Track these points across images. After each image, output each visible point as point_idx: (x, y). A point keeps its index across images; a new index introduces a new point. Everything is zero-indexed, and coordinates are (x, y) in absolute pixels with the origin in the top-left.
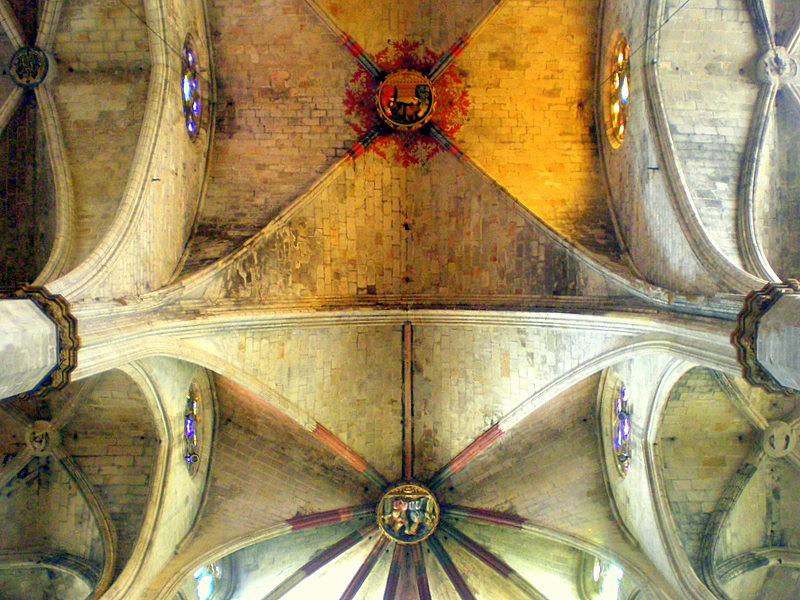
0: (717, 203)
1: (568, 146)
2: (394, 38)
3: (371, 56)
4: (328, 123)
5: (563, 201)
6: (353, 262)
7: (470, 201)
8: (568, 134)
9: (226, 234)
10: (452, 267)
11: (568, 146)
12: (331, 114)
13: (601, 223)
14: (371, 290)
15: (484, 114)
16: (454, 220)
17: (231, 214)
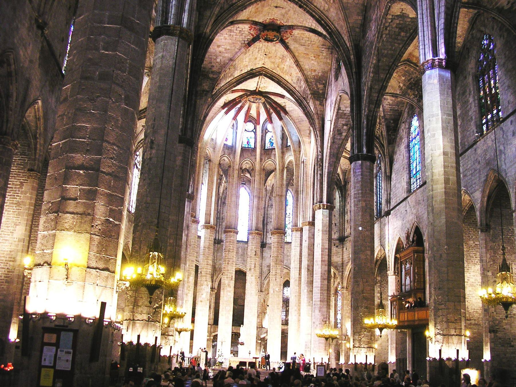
0: (340, 134)
1: (323, 49)
2: (268, 18)
3: (260, 23)
4: (243, 32)
5: (315, 71)
6: (247, 66)
7: (287, 59)
8: (325, 46)
9: (208, 76)
10: (278, 69)
11: (323, 49)
12: (244, 30)
13: (324, 82)
14: (252, 70)
15: (298, 36)
16: (281, 59)
17: (209, 65)
